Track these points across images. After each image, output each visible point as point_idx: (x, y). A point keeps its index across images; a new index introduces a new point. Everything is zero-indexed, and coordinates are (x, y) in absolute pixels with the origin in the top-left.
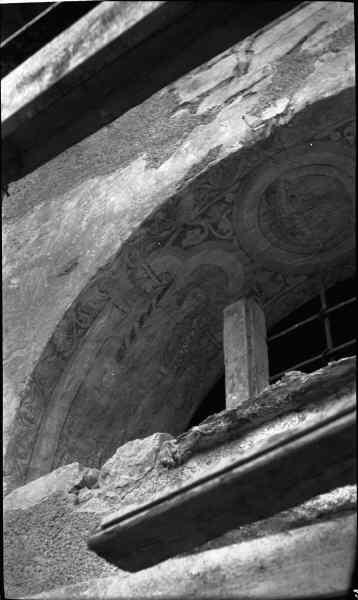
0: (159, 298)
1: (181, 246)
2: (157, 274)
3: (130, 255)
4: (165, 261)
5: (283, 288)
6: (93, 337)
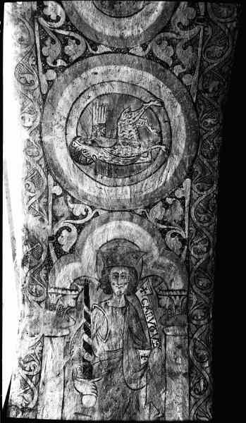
0: (87, 302)
1: (65, 254)
2: (68, 288)
3: (31, 293)
4: (64, 275)
5: (183, 204)
6: (50, 375)
